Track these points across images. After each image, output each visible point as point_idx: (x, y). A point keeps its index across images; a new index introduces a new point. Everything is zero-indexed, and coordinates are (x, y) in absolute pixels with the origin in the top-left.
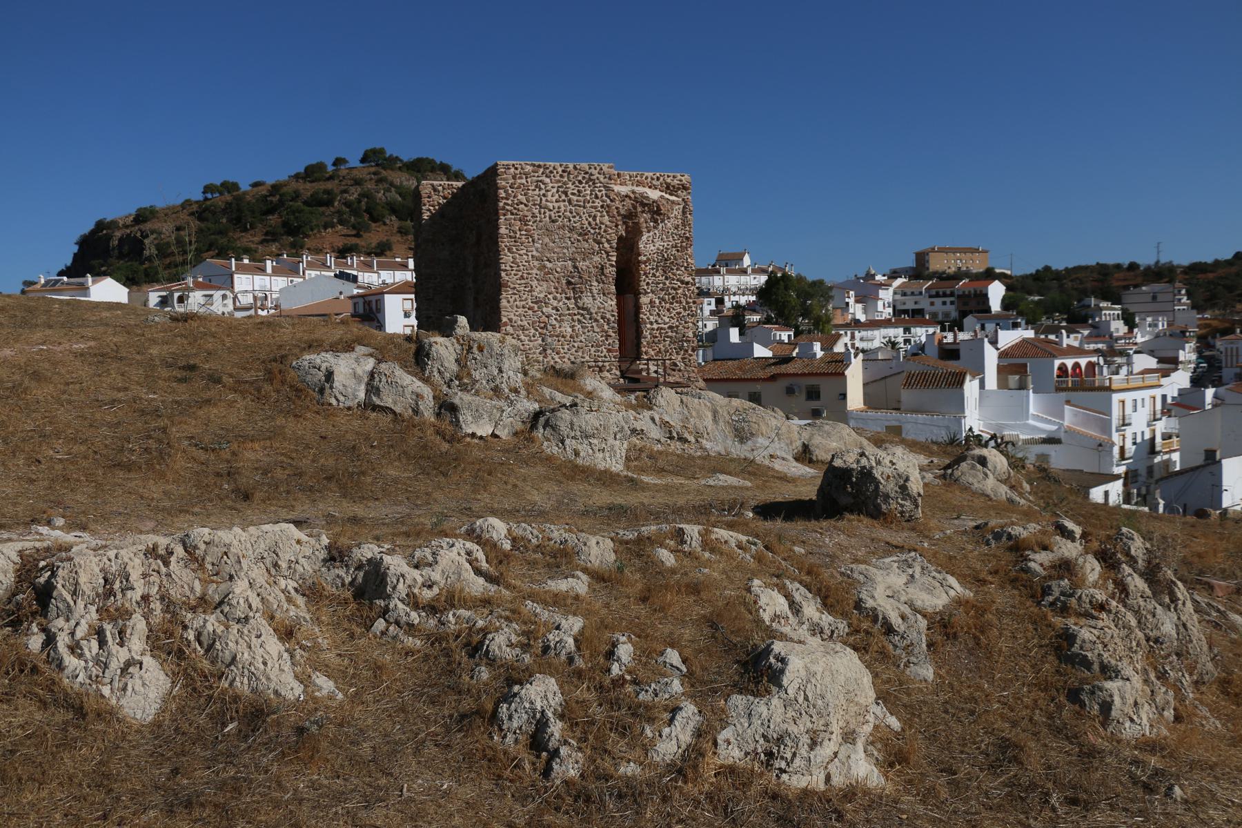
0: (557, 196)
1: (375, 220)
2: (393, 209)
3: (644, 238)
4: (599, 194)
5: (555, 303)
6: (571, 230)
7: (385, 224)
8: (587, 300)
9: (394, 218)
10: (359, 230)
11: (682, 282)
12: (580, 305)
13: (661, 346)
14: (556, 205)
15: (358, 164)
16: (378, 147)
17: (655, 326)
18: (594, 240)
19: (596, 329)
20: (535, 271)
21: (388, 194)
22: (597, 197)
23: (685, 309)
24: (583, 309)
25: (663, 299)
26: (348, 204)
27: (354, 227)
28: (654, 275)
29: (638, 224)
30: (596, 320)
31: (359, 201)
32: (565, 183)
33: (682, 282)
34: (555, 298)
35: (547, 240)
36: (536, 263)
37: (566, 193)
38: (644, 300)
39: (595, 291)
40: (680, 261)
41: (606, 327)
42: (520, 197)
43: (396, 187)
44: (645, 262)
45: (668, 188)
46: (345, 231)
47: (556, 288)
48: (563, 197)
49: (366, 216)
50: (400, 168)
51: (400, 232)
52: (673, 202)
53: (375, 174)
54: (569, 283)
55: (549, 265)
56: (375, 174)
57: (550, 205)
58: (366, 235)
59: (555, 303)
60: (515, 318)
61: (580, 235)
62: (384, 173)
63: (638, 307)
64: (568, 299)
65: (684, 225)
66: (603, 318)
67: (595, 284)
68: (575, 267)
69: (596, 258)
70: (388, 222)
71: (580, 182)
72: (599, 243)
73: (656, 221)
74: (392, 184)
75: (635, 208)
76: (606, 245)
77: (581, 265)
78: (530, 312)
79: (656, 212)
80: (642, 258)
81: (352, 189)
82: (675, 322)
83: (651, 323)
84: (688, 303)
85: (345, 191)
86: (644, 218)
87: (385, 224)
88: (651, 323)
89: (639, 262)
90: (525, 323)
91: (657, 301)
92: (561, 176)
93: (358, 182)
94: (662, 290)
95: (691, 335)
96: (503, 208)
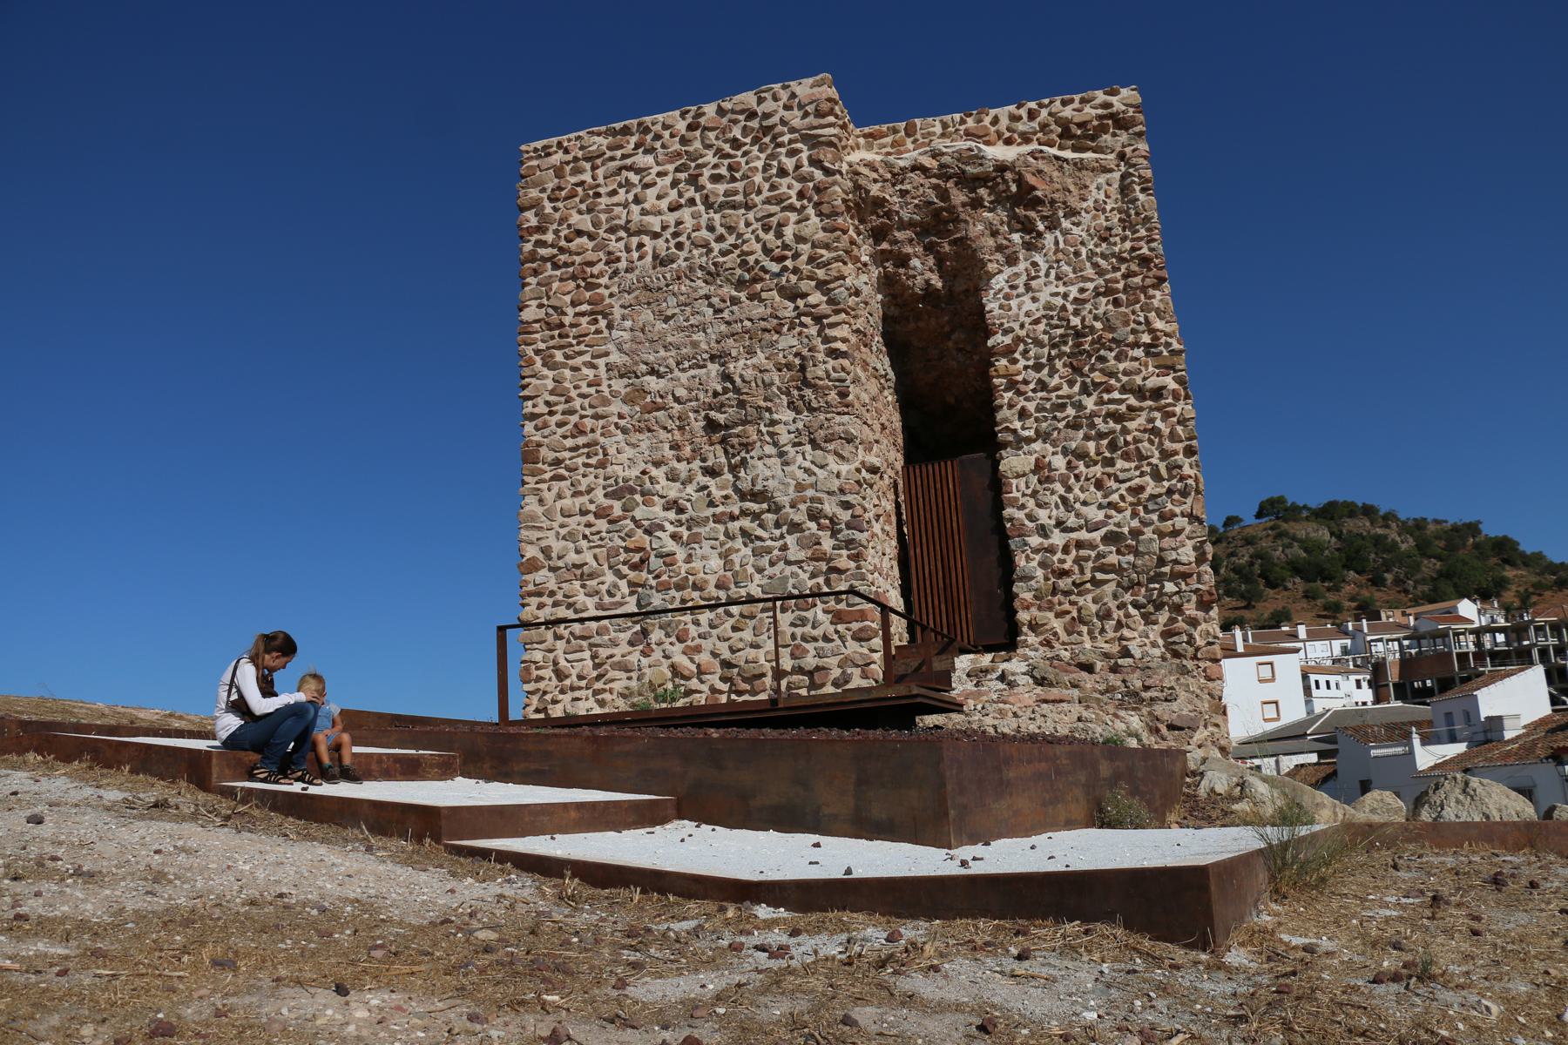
0: (674, 194)
1: (1272, 585)
2: (1296, 569)
3: (999, 282)
4: (789, 163)
5: (673, 491)
6: (711, 276)
7: (1286, 589)
8: (764, 470)
9: (1298, 580)
10: (1249, 600)
11: (1140, 393)
12: (745, 485)
13: (1087, 601)
14: (671, 218)
15: (1254, 521)
16: (1276, 495)
17: (1058, 538)
18: (782, 290)
19: (795, 553)
20: (616, 407)
21: (1288, 551)
22: (783, 172)
23: (1157, 477)
24: (757, 496)
25: (1081, 455)
26: (1237, 570)
27: (1242, 597)
28: (1042, 385)
29: (962, 243)
30: (795, 527)
31: (1252, 564)
32: (693, 157)
33: (1140, 393)
34: (672, 477)
35: (647, 315)
36: (619, 385)
37: (693, 180)
38: (1013, 462)
39: (784, 438)
40: (1123, 332)
41: (827, 544)
42: (575, 218)
43: (1300, 541)
44: (1008, 352)
45: (1066, 134)
46: (1235, 604)
47: (675, 446)
48: (691, 192)
49: (1262, 582)
50: (1307, 518)
51: (1306, 597)
52: (1079, 166)
53: (1272, 528)
54: (712, 426)
55: (652, 383)
56: (1272, 528)
57: (655, 223)
58: (1259, 605)
59: (673, 491)
60: (557, 546)
61: (740, 284)
62: (1285, 526)
63: (997, 484)
64: (712, 472)
65: (1127, 223)
66: (814, 516)
67: (787, 415)
68: (726, 377)
69: (788, 341)
70: (1290, 585)
71: (736, 144)
72: (793, 295)
73: (1027, 227)
74: (1294, 538)
75: (944, 195)
76: (816, 298)
77: (739, 368)
78: (602, 525)
79: (1021, 199)
80: (998, 340)
81: (1243, 551)
82: (1125, 521)
83: (1043, 531)
84: (1165, 455)
85: (1232, 554)
86: (983, 226)
87: (1286, 589)
88: (1043, 531)
89: (992, 352)
90: (588, 557)
91: (1059, 462)
92: (684, 141)
93: (1249, 541)
94: (1074, 425)
95: (1187, 554)
96: (533, 257)
